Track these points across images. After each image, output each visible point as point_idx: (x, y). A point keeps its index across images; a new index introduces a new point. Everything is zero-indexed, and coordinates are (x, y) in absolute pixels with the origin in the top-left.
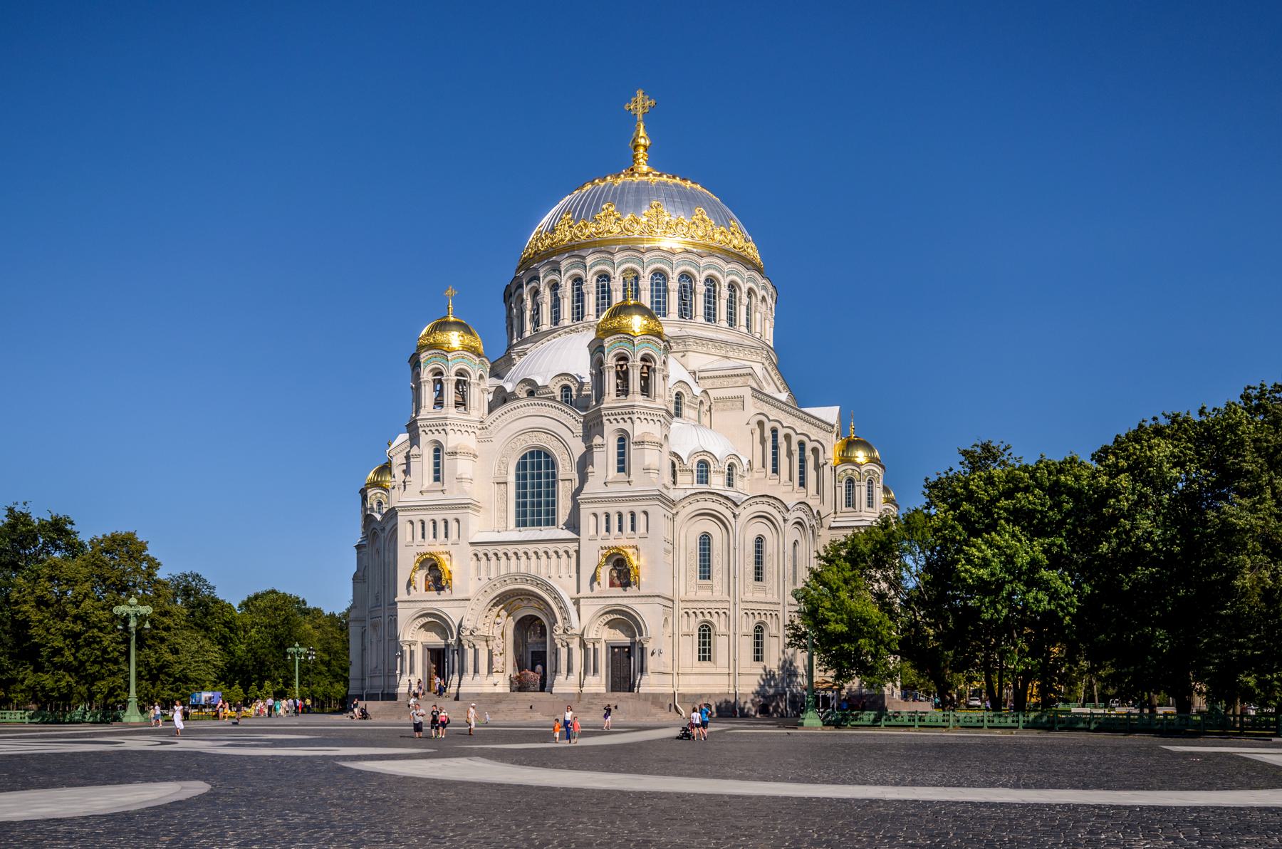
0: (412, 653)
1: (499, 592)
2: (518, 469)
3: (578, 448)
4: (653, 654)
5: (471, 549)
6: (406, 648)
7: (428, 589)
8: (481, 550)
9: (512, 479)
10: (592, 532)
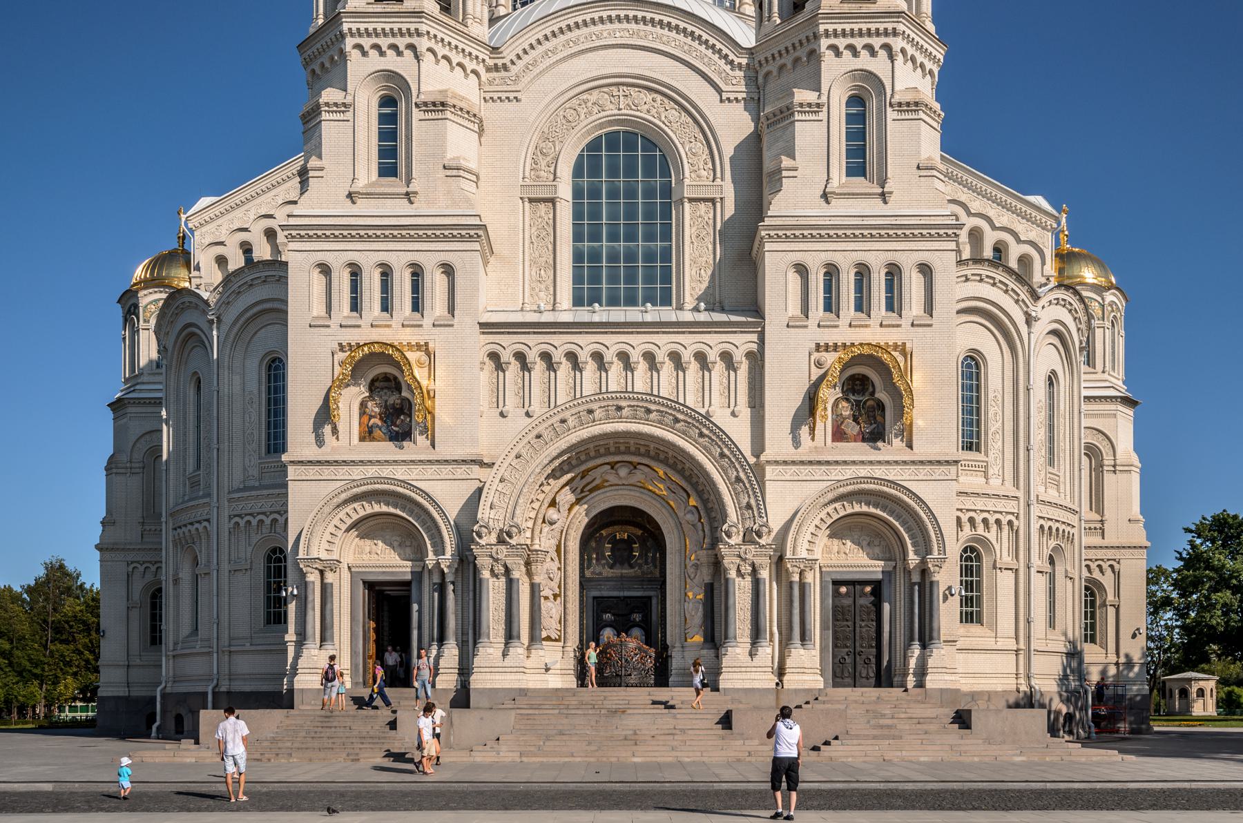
0: (325, 588)
1: (573, 438)
2: (577, 172)
3: (734, 124)
4: (945, 598)
5: (482, 344)
6: (314, 577)
7: (368, 434)
8: (508, 344)
9: (565, 191)
10: (794, 309)
